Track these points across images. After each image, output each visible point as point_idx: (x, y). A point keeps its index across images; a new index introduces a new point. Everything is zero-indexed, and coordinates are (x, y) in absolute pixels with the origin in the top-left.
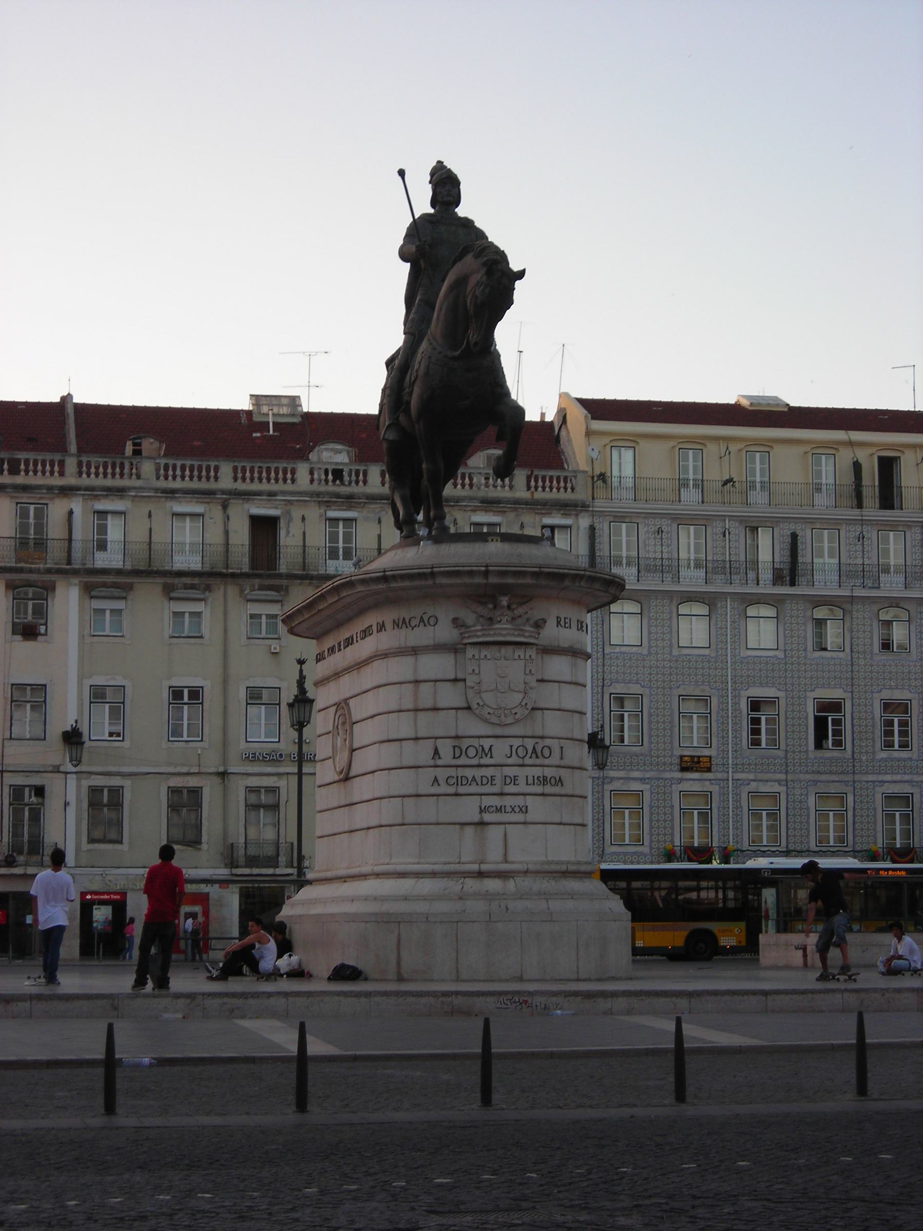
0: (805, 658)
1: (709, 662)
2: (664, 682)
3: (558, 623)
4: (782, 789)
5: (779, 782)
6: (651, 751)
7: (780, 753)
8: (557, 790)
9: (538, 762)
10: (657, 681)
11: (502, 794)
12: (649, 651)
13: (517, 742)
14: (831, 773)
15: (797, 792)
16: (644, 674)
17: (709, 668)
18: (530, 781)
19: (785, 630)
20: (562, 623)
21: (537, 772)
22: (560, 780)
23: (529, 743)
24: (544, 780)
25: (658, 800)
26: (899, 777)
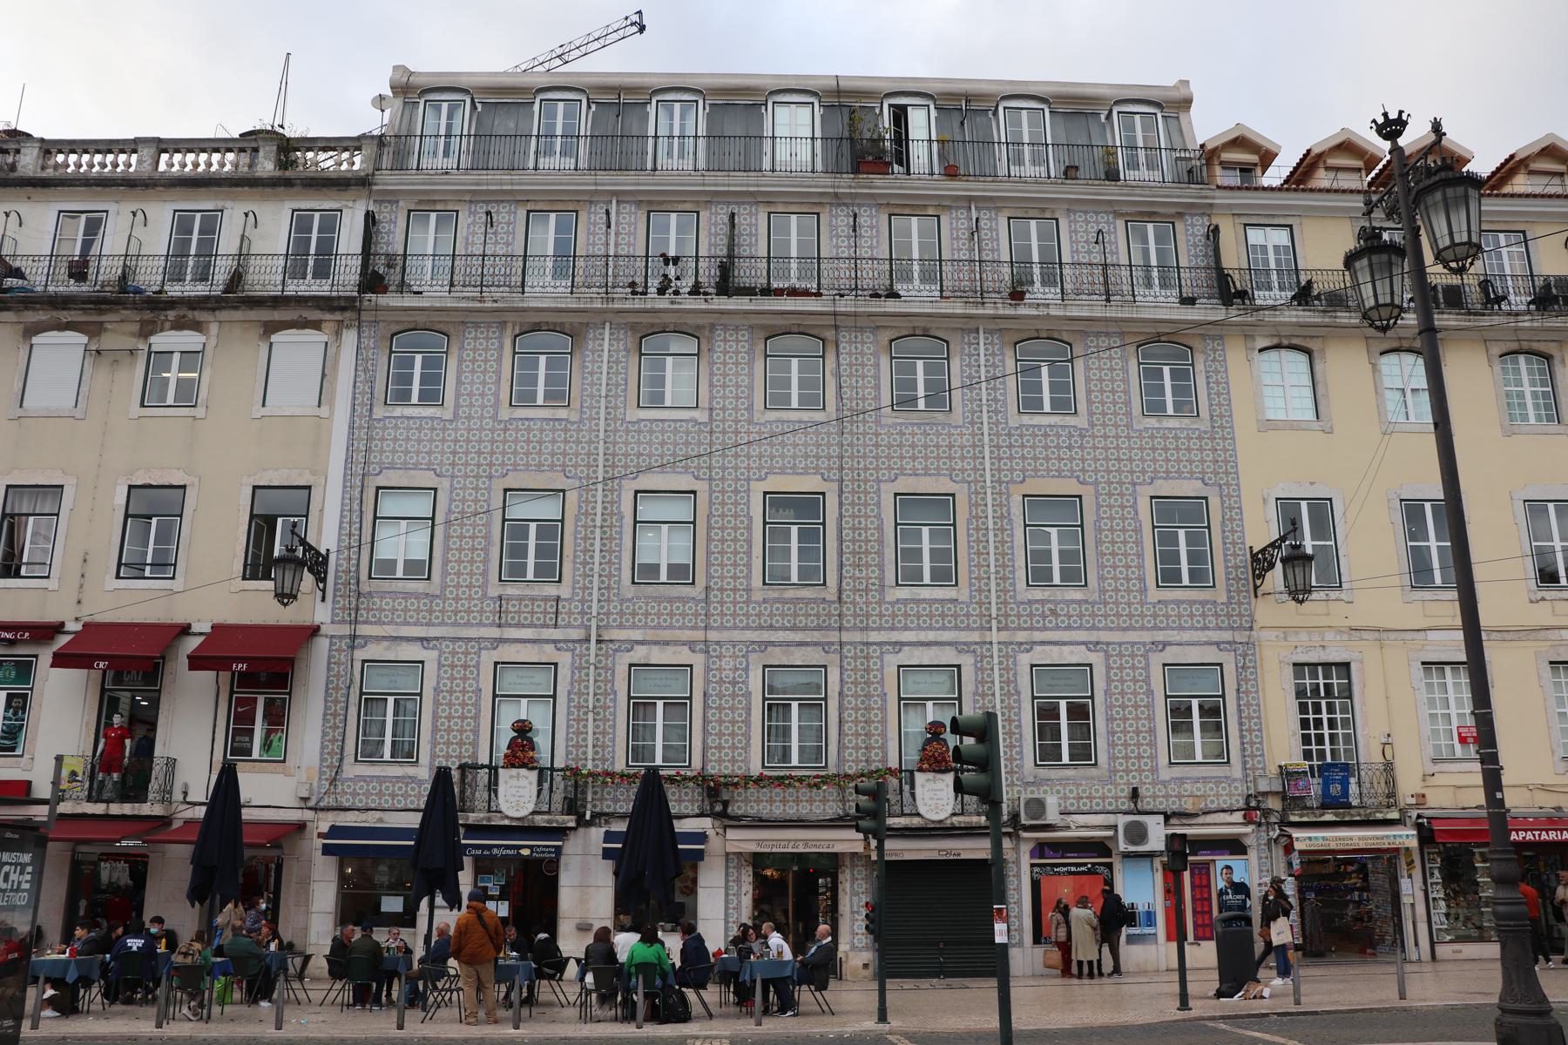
0: (750, 421)
1: (566, 430)
2: (479, 465)
4: (698, 660)
5: (691, 645)
6: (444, 587)
7: (697, 591)
10: (466, 464)
12: (456, 414)
14: (794, 628)
15: (728, 663)
16: (442, 453)
17: (566, 441)
19: (712, 374)
25: (452, 678)
26: (931, 636)
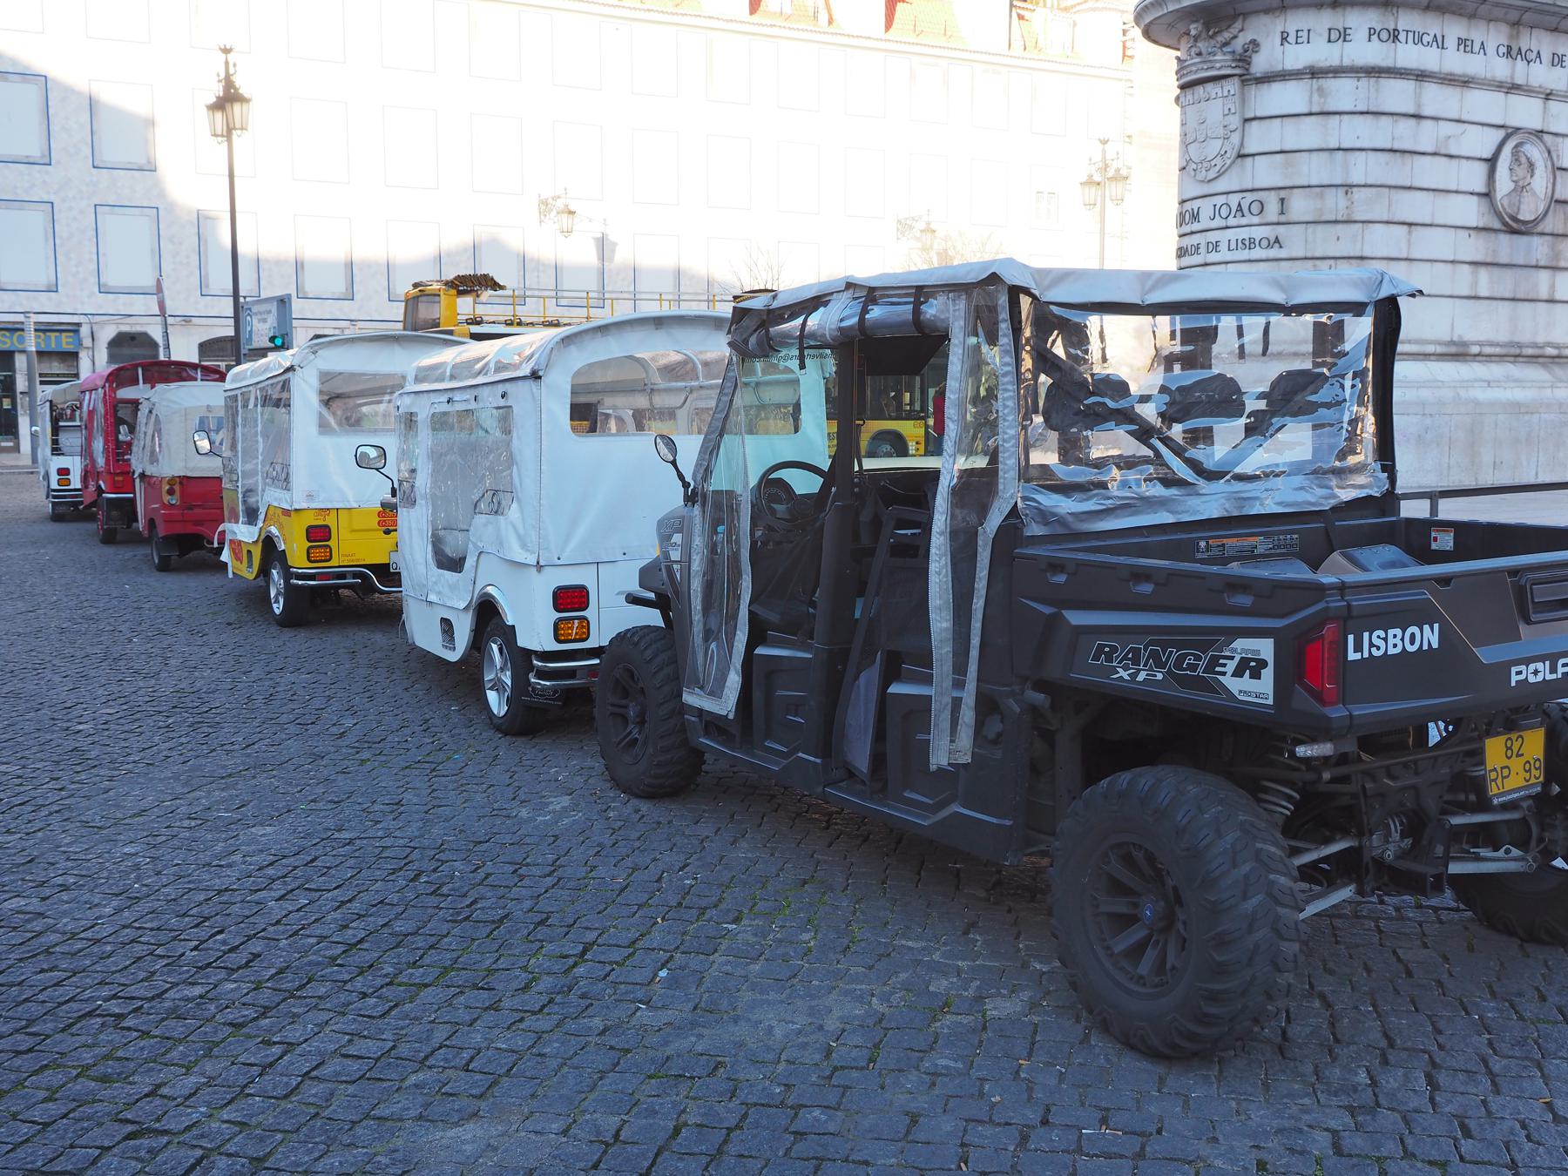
3: (1284, 39)
8: (1274, 253)
9: (1244, 221)
11: (1206, 264)
13: (1220, 200)
18: (1233, 246)
20: (1292, 39)
21: (1244, 233)
22: (1277, 240)
23: (1234, 200)
24: (1250, 244)
